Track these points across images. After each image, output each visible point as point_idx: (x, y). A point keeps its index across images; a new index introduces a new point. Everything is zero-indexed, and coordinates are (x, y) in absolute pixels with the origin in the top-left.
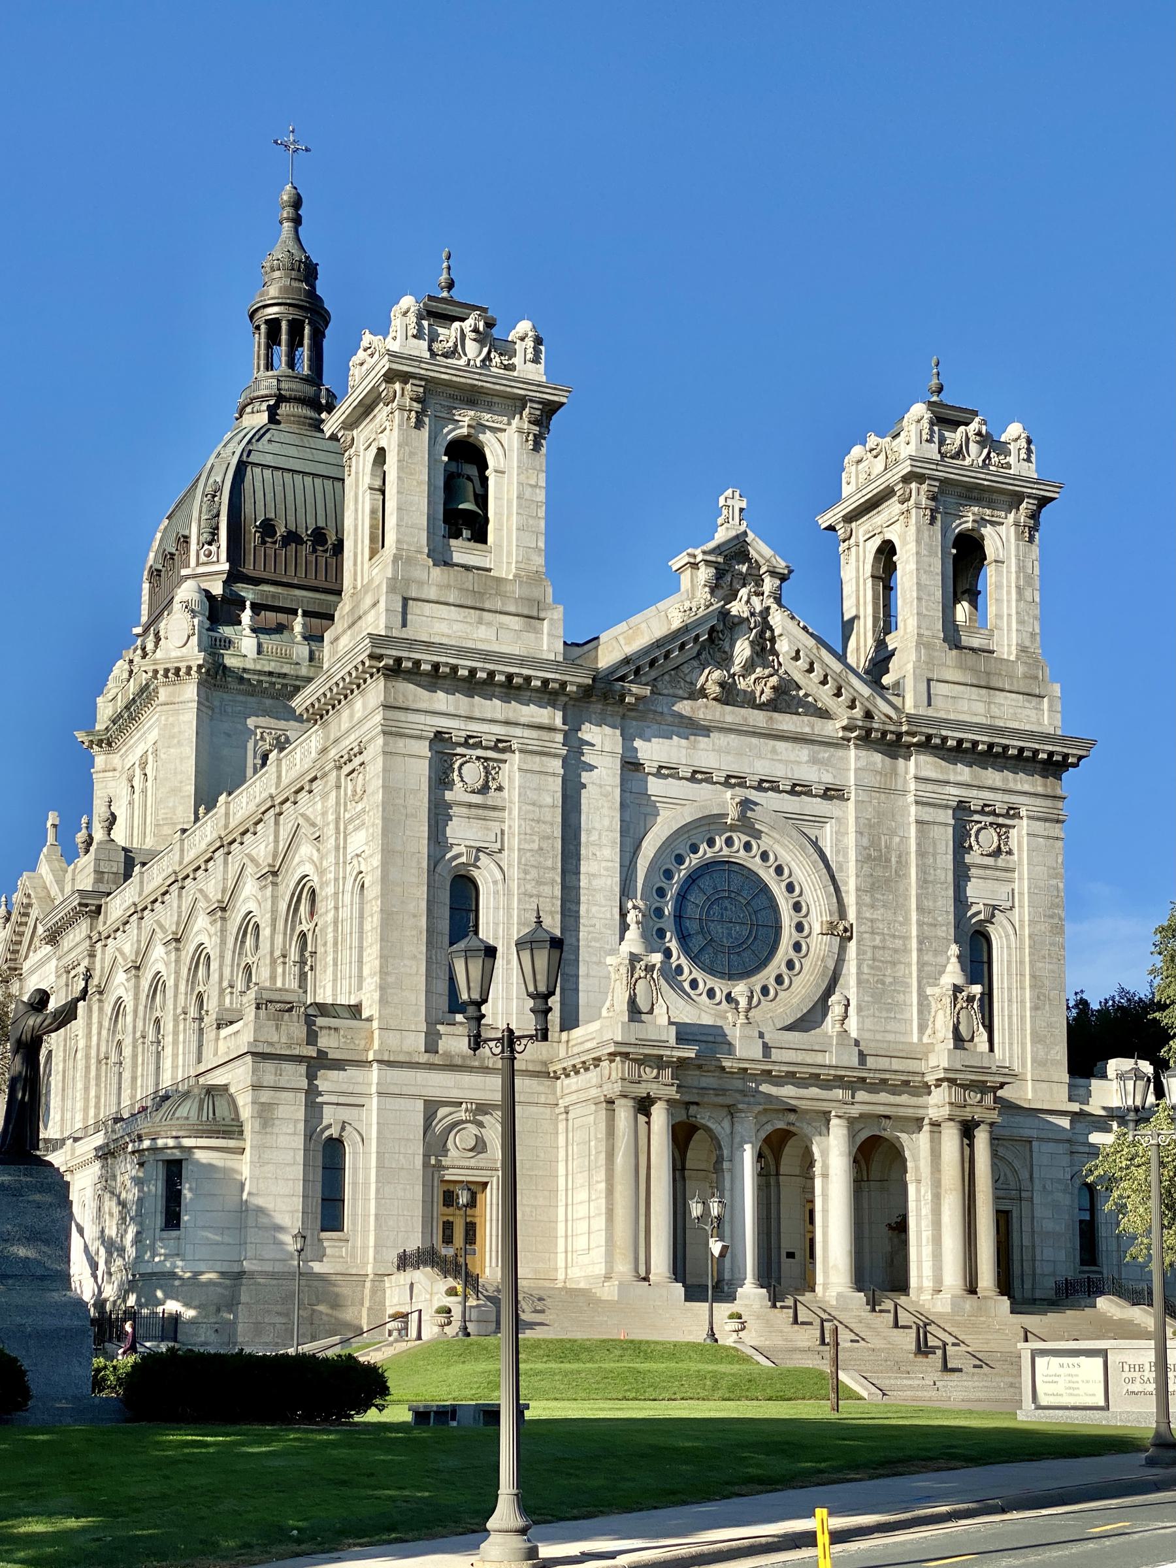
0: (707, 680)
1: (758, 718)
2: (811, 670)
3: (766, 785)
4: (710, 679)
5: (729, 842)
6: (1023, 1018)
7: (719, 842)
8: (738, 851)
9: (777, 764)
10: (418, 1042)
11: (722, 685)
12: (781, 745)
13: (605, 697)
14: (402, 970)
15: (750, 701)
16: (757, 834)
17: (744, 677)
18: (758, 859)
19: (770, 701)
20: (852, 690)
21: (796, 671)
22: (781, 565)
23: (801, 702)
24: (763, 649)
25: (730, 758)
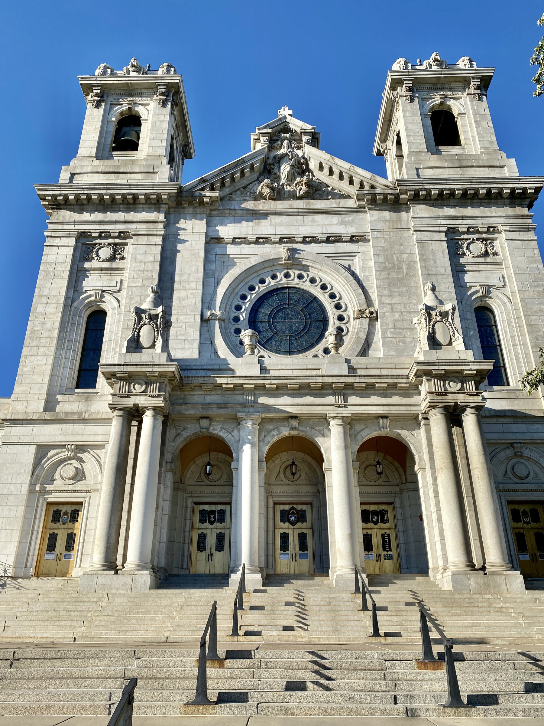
0: (262, 188)
1: (301, 204)
2: (331, 173)
3: (308, 239)
4: (263, 187)
5: (287, 276)
6: (527, 355)
7: (280, 275)
8: (293, 279)
9: (315, 227)
10: (41, 405)
11: (272, 189)
12: (318, 218)
13: (190, 204)
14: (36, 363)
15: (293, 196)
16: (306, 268)
17: (290, 186)
18: (308, 283)
19: (306, 192)
20: (359, 176)
21: (322, 177)
22: (309, 128)
23: (329, 193)
24: (301, 167)
25: (282, 228)
